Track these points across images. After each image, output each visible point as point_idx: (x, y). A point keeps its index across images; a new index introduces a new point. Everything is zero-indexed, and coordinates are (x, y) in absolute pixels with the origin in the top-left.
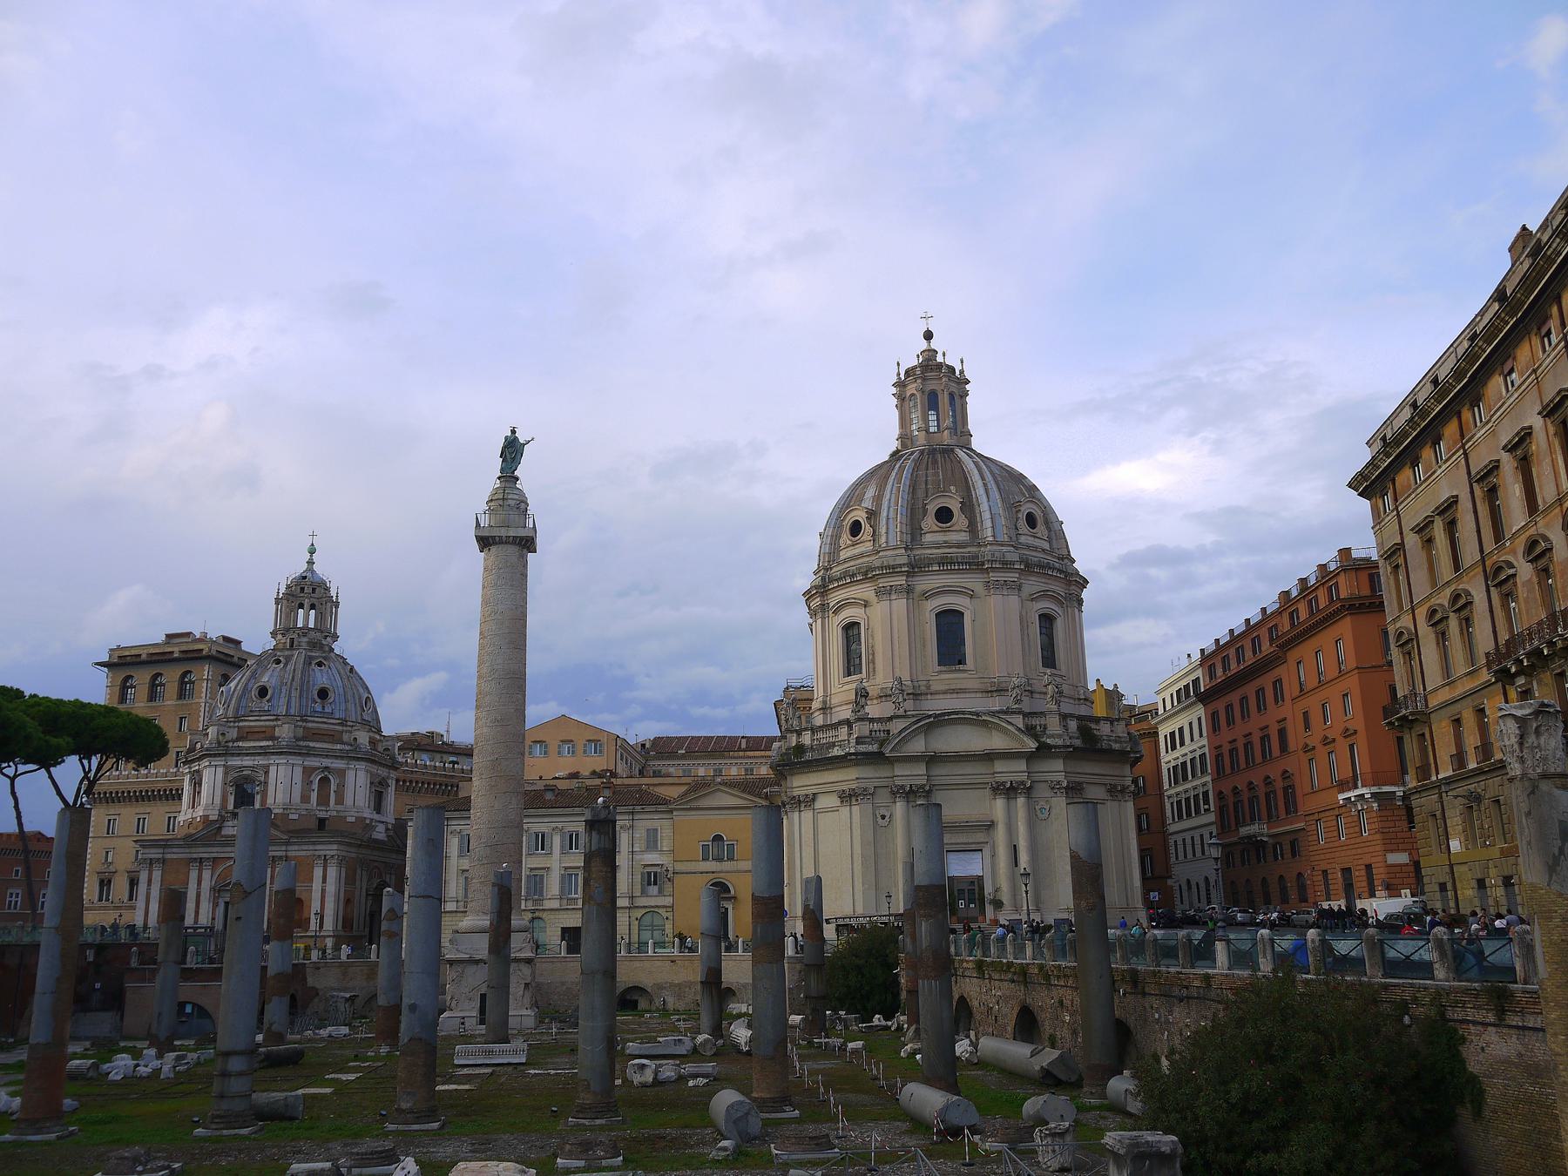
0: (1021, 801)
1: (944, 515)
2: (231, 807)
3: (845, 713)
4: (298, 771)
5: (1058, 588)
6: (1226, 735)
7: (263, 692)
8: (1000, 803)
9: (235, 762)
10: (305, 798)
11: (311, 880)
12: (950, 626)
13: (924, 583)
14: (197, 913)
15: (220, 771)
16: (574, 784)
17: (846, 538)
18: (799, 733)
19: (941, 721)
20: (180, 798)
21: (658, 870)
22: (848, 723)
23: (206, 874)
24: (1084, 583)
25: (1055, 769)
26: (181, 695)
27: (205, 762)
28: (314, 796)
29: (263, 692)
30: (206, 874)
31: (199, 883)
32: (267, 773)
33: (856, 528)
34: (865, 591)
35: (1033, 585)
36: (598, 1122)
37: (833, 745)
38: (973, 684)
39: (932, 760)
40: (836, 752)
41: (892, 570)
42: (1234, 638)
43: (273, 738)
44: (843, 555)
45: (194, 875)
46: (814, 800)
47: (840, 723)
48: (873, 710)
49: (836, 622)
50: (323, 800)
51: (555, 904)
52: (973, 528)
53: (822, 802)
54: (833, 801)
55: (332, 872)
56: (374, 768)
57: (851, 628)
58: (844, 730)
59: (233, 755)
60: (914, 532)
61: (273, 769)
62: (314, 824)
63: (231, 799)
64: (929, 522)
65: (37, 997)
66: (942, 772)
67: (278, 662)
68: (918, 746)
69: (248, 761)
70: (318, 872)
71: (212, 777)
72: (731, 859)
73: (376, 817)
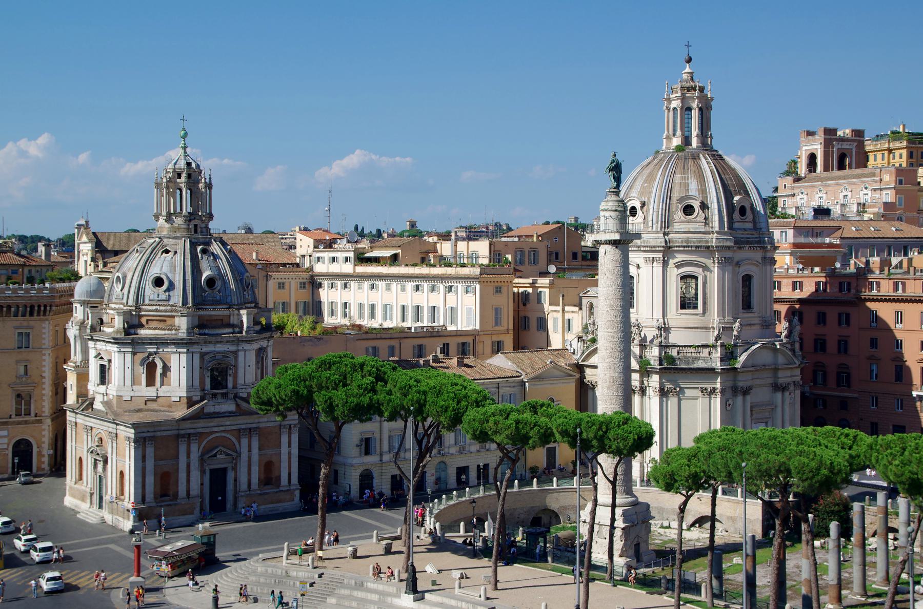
0: (787, 394)
5: (758, 255)
8: (779, 395)
14: (188, 481)
17: (679, 215)
23: (194, 448)
31: (188, 456)
32: (236, 358)
37: (697, 359)
38: (756, 321)
40: (700, 364)
44: (677, 227)
45: (183, 448)
54: (697, 393)
55: (295, 438)
61: (241, 354)
64: (736, 215)
70: (284, 439)
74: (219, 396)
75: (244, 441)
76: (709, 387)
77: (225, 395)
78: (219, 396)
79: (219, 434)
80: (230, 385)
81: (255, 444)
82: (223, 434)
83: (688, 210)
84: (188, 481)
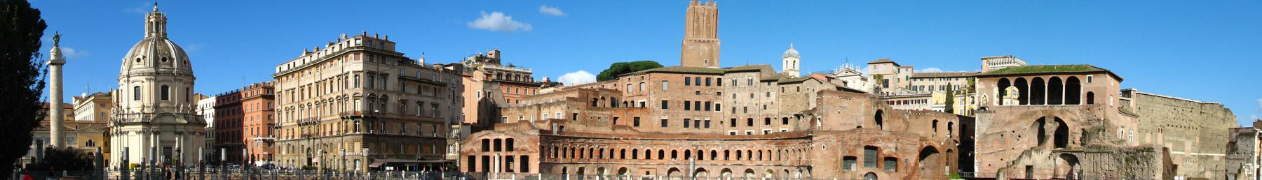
1: (164, 60)
3: (139, 110)
6: (221, 119)
12: (165, 89)
13: (160, 78)
17: (135, 62)
19: (164, 114)
24: (194, 78)
25: (191, 128)
33: (138, 60)
34: (143, 78)
35: (186, 79)
39: (161, 124)
41: (151, 74)
42: (227, 95)
48: (146, 111)
49: (132, 86)
52: (171, 64)
57: (137, 88)
60: (156, 64)
66: (164, 128)
68: (158, 121)
83: (138, 60)
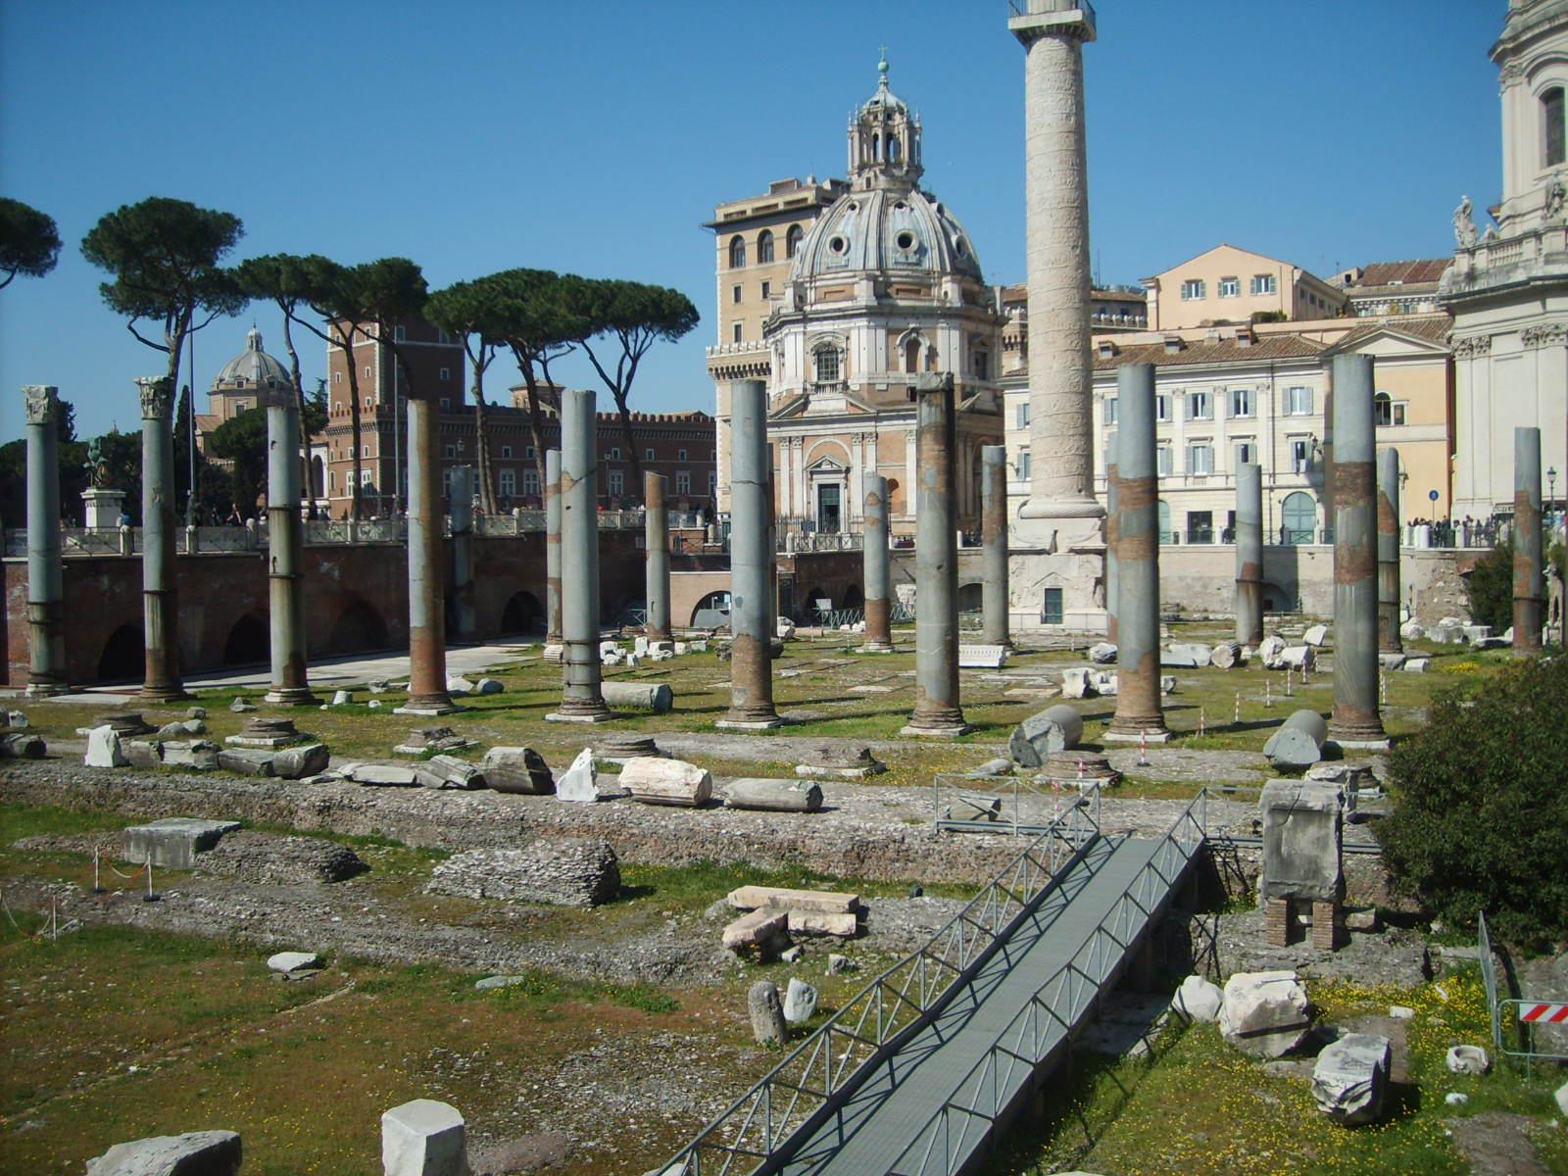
2: (815, 379)
4: (882, 333)
7: (837, 244)
9: (814, 327)
10: (890, 365)
11: (904, 459)
14: (791, 497)
15: (800, 338)
16: (1204, 334)
18: (1472, 252)
20: (770, 370)
21: (1305, 439)
22: (1537, 235)
23: (797, 454)
26: (761, 259)
27: (785, 330)
28: (902, 362)
29: (837, 244)
30: (797, 454)
36: (935, 732)
37: (1516, 266)
40: (1519, 276)
43: (852, 298)
46: (1489, 345)
47: (1526, 236)
50: (911, 367)
51: (1179, 483)
53: (1500, 346)
54: (1513, 344)
56: (971, 326)
58: (1529, 248)
59: (812, 320)
61: (854, 335)
62: (903, 395)
63: (815, 368)
65: (411, 584)
67: (853, 207)
69: (827, 326)
71: (795, 345)
72: (1400, 422)
73: (978, 383)
74: (828, 389)
75: (858, 449)
76: (1530, 324)
77: (833, 387)
78: (828, 389)
79: (827, 439)
80: (841, 377)
81: (871, 450)
82: (832, 439)
84: (791, 497)
